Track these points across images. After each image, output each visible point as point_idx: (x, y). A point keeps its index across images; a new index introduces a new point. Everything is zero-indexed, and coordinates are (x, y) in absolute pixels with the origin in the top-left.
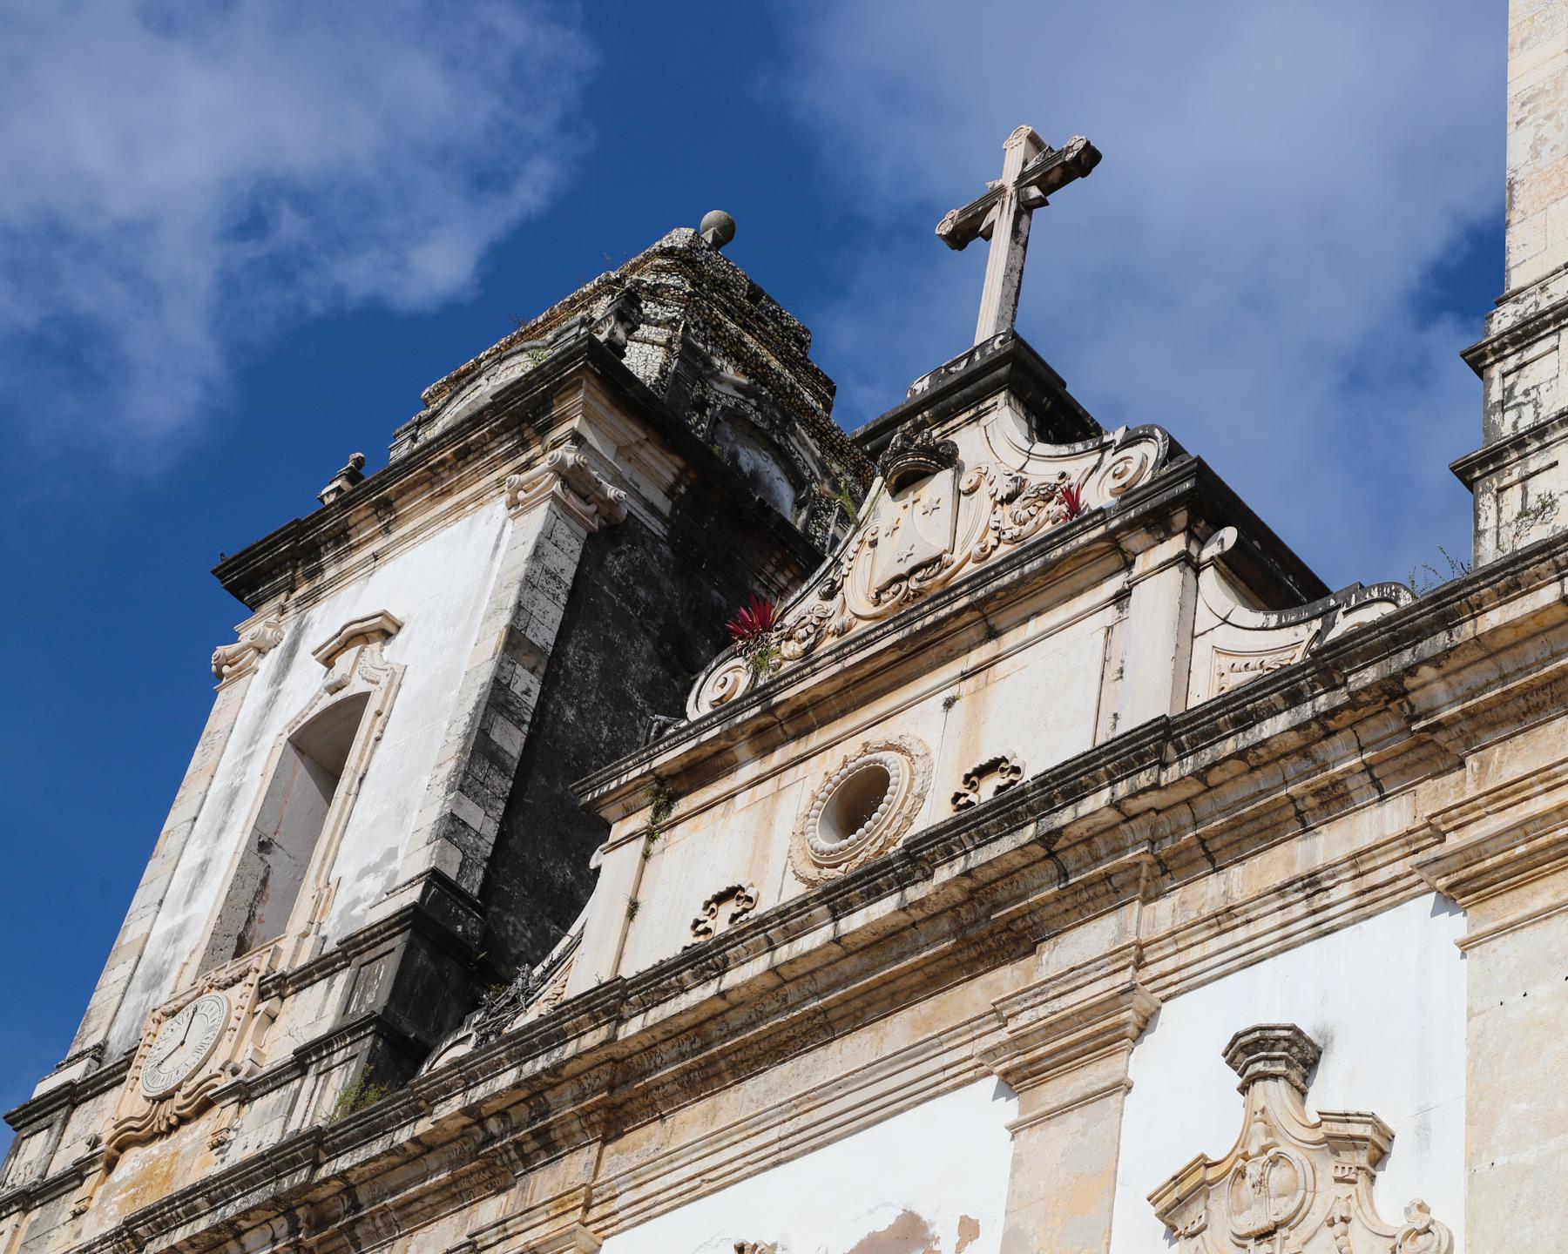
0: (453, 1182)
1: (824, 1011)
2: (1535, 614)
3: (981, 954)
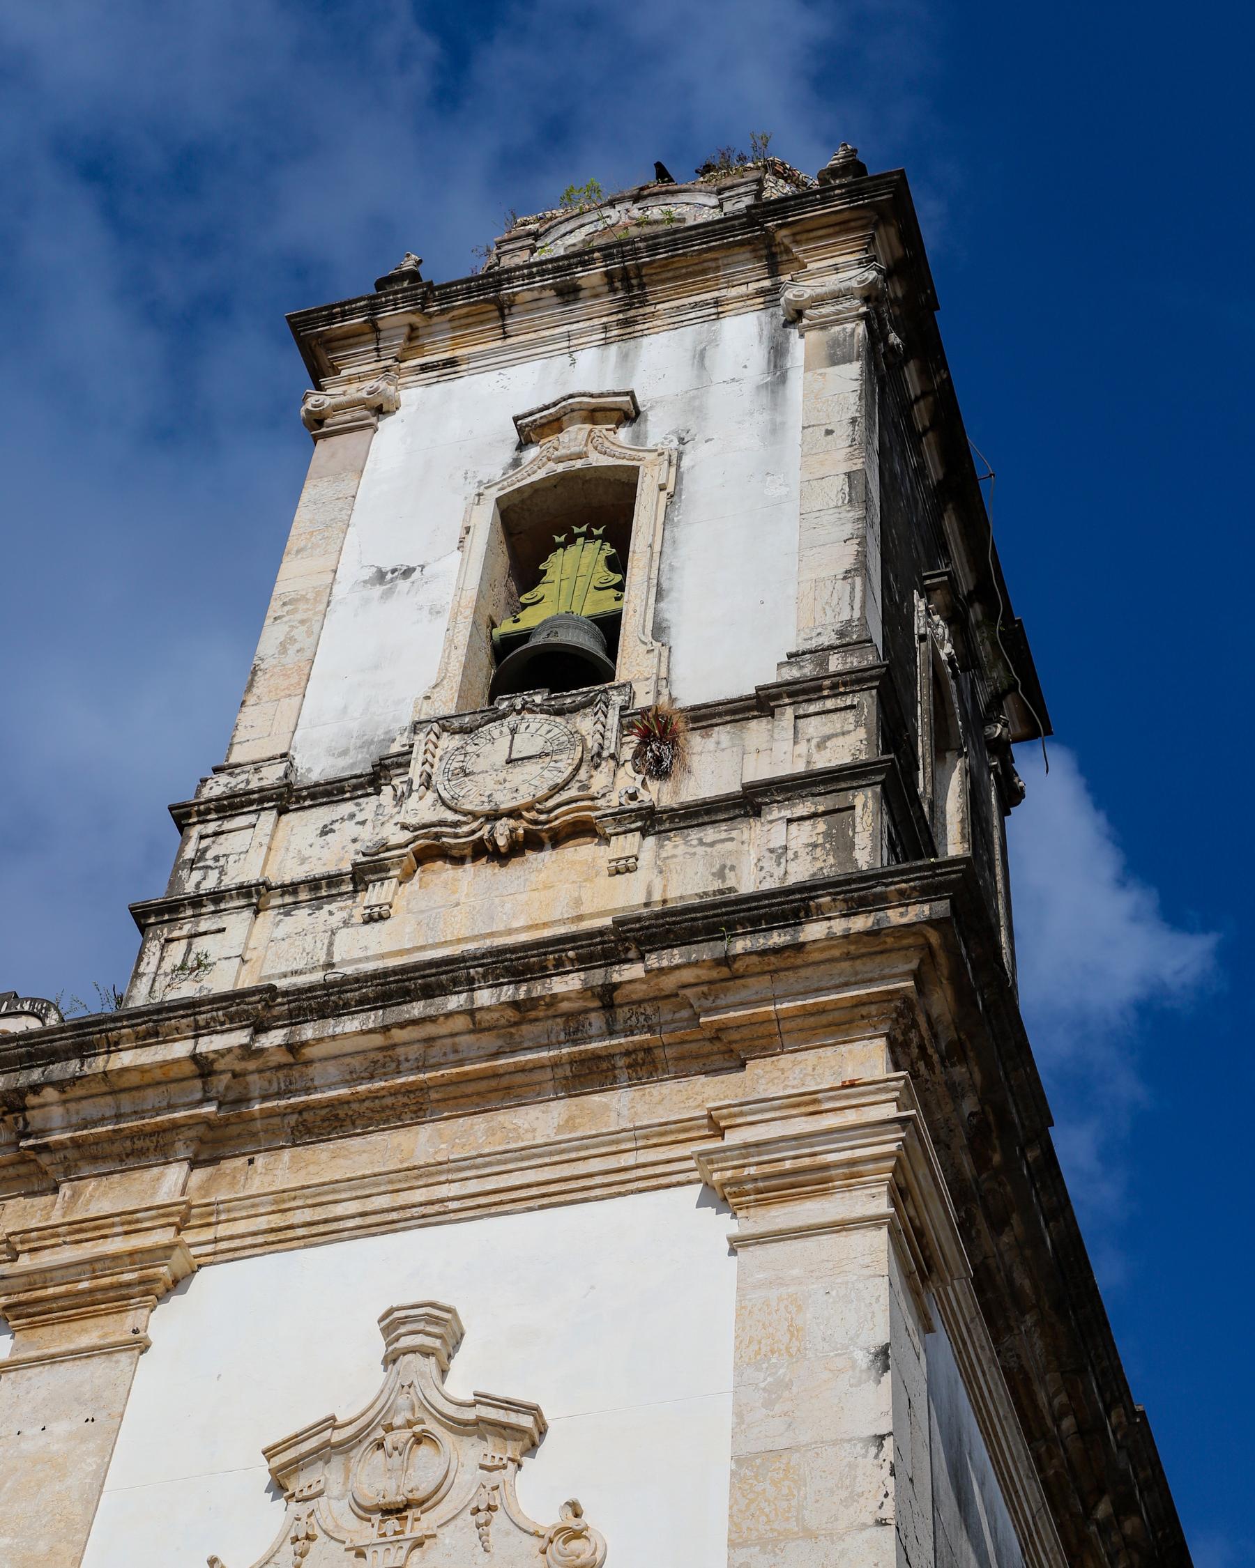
2: (164, 1064)
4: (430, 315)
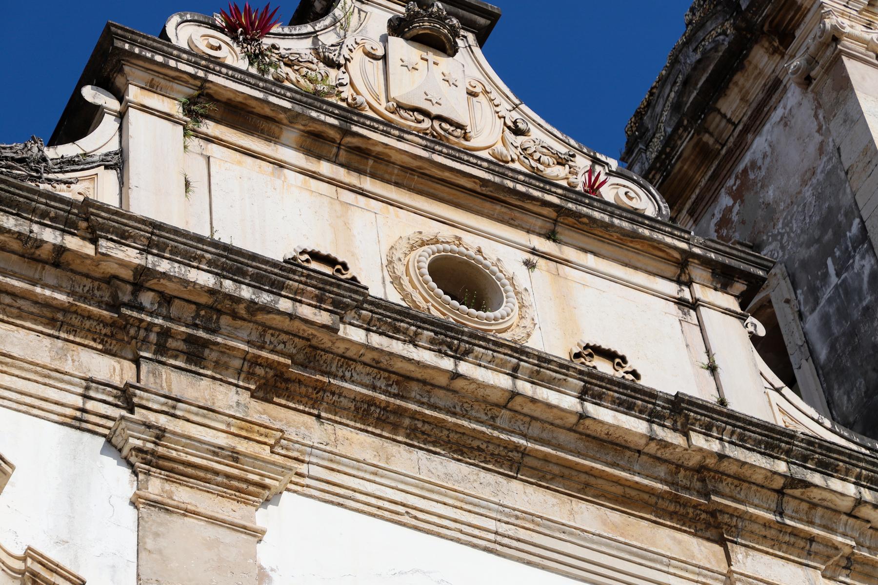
0: (65, 310)
3: (676, 513)
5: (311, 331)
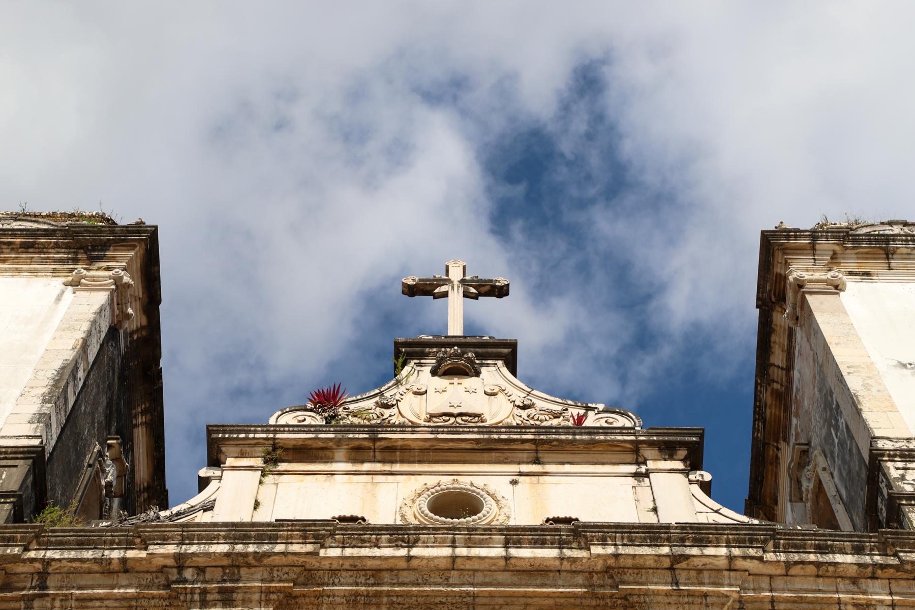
1: (474, 596)
4: (847, 248)
5: (302, 560)
